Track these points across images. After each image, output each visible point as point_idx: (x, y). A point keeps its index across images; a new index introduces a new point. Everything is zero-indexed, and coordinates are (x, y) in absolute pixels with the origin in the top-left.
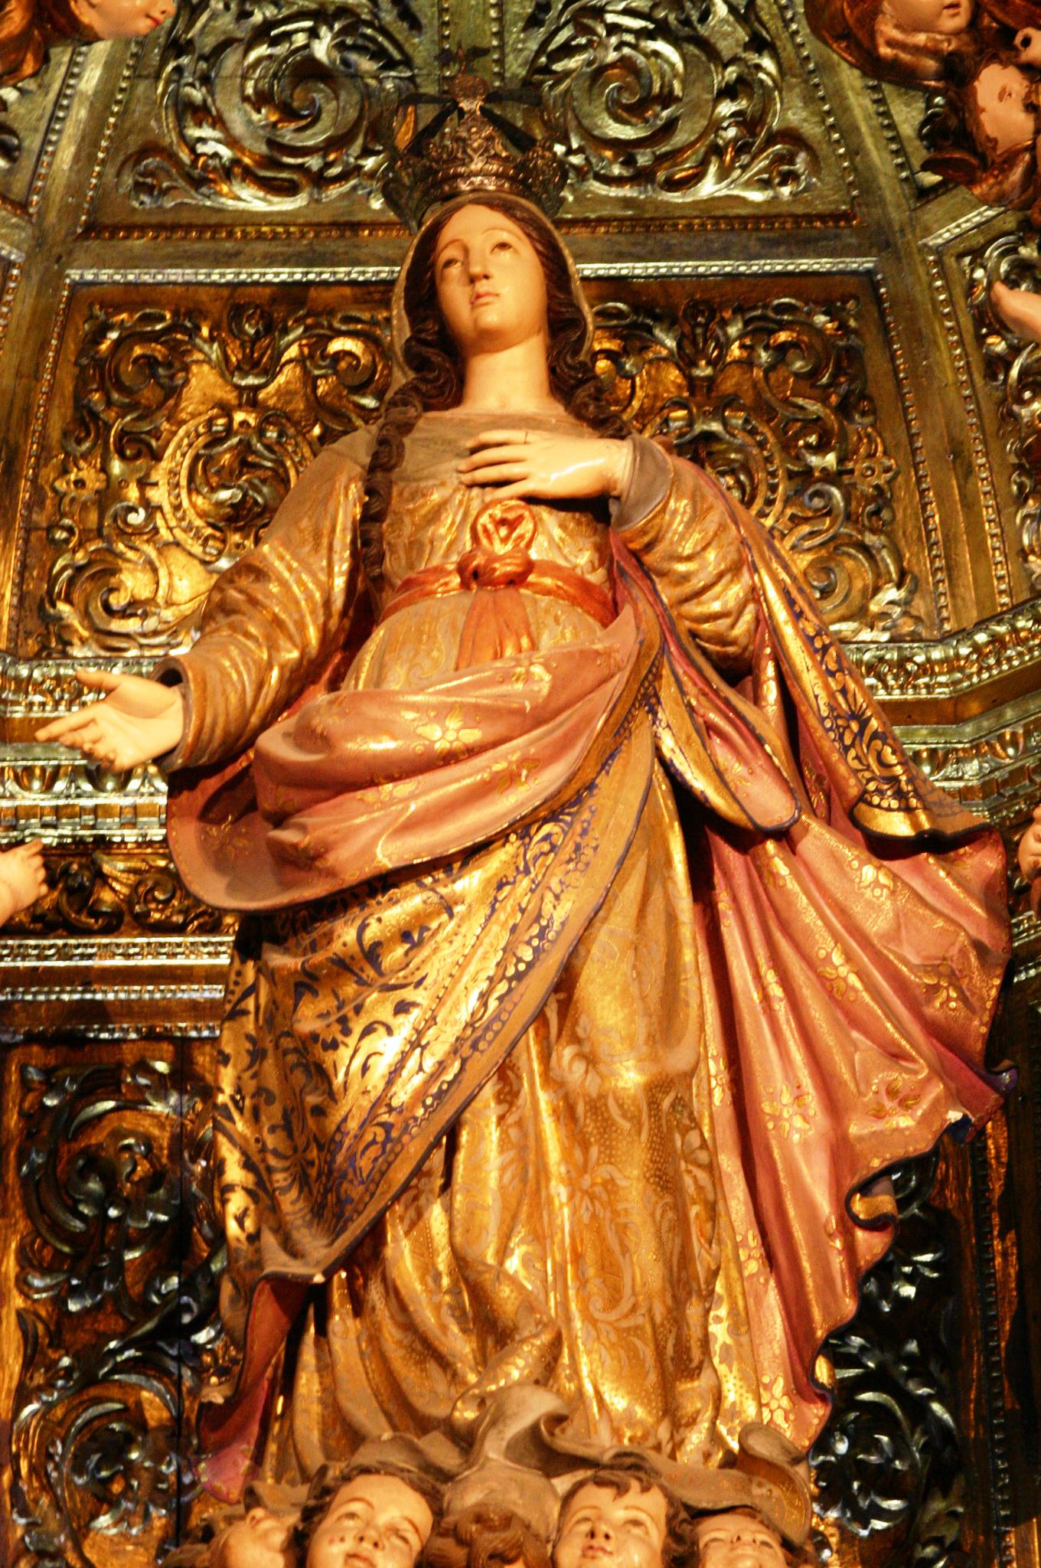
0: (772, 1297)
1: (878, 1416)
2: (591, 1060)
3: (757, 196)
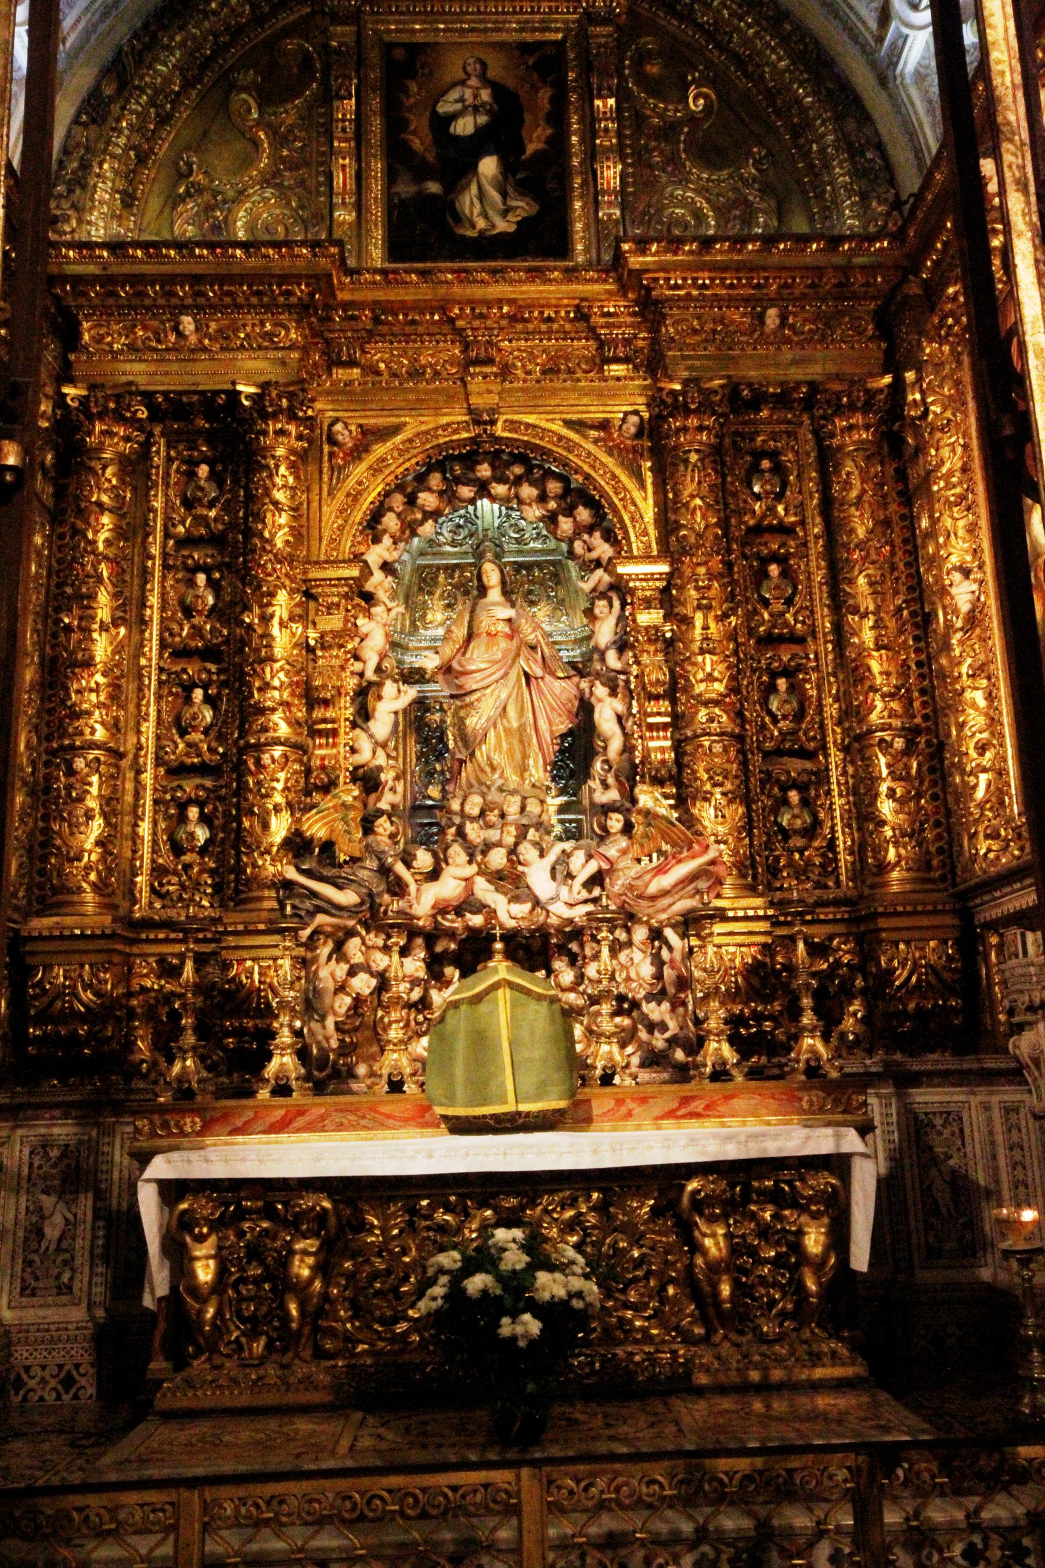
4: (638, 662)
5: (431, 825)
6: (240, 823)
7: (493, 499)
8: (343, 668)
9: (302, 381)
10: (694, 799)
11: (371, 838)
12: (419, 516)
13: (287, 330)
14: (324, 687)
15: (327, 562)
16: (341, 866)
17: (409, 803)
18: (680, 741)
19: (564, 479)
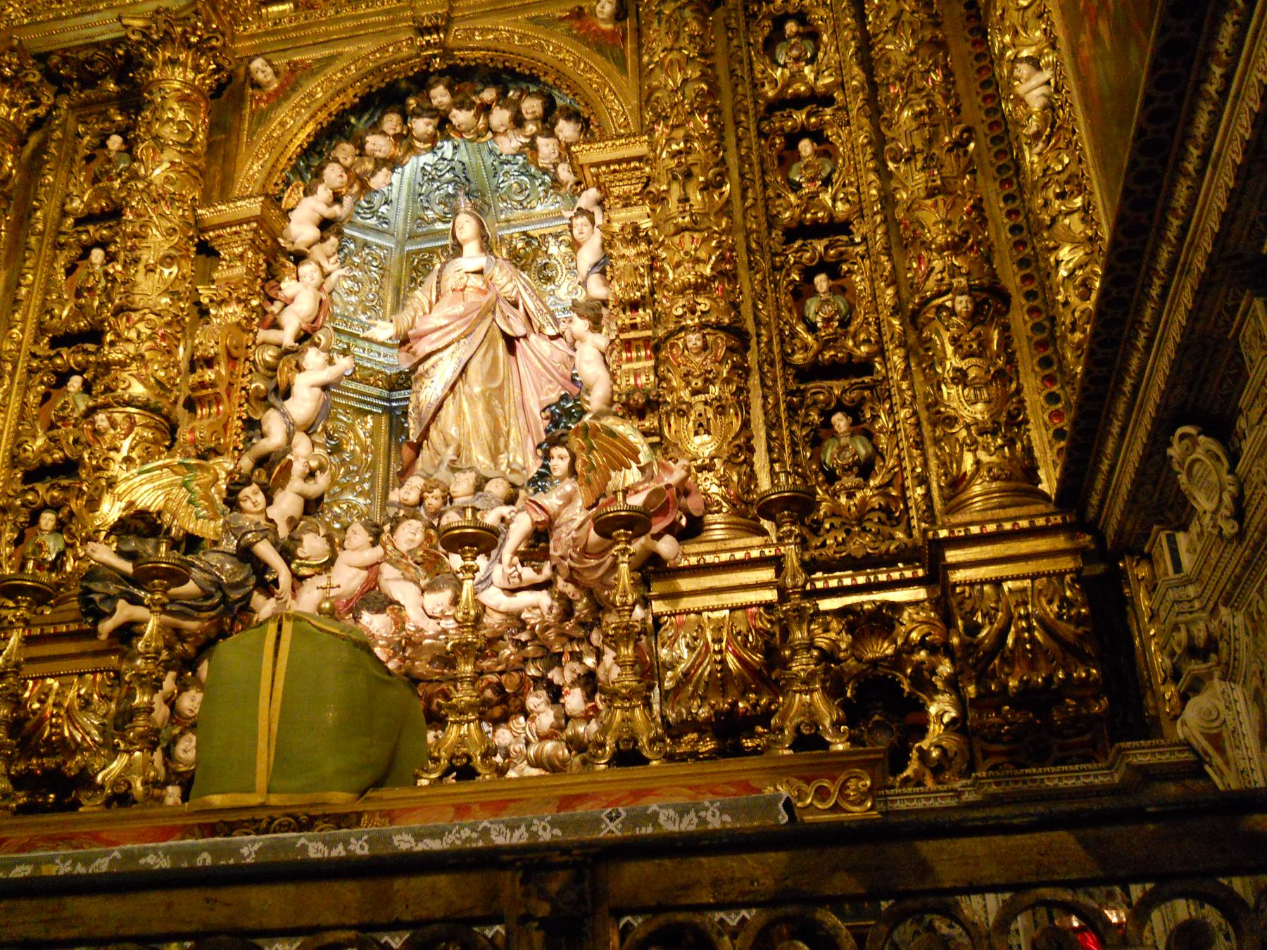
3: (552, 208)
12: (370, 166)
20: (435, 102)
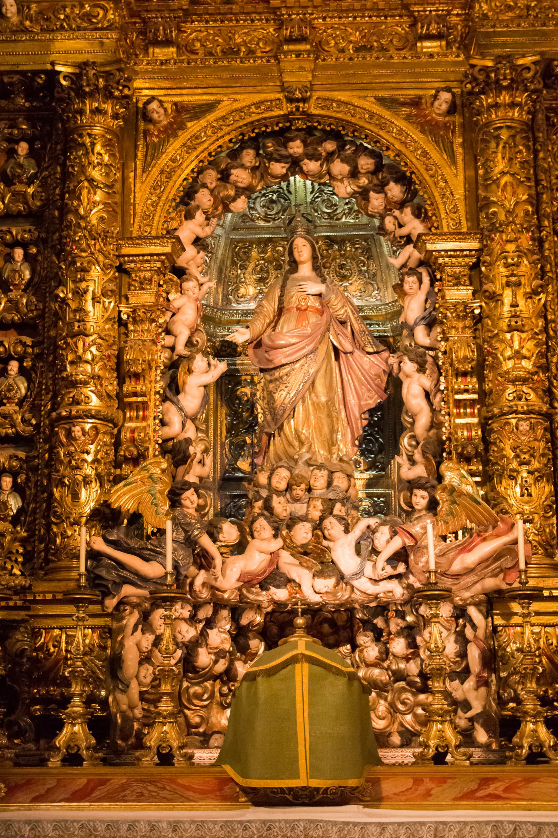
0: (349, 430)
1: (370, 441)
2: (317, 397)
4: (446, 339)
5: (240, 497)
6: (51, 494)
7: (305, 175)
8: (154, 342)
9: (120, 61)
10: (501, 476)
11: (178, 511)
12: (232, 193)
13: (106, 11)
14: (135, 360)
15: (140, 238)
16: (148, 538)
17: (218, 475)
18: (487, 419)
19: (377, 156)
20: (291, 151)
